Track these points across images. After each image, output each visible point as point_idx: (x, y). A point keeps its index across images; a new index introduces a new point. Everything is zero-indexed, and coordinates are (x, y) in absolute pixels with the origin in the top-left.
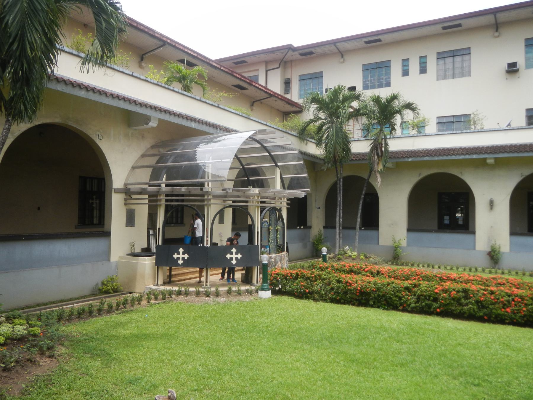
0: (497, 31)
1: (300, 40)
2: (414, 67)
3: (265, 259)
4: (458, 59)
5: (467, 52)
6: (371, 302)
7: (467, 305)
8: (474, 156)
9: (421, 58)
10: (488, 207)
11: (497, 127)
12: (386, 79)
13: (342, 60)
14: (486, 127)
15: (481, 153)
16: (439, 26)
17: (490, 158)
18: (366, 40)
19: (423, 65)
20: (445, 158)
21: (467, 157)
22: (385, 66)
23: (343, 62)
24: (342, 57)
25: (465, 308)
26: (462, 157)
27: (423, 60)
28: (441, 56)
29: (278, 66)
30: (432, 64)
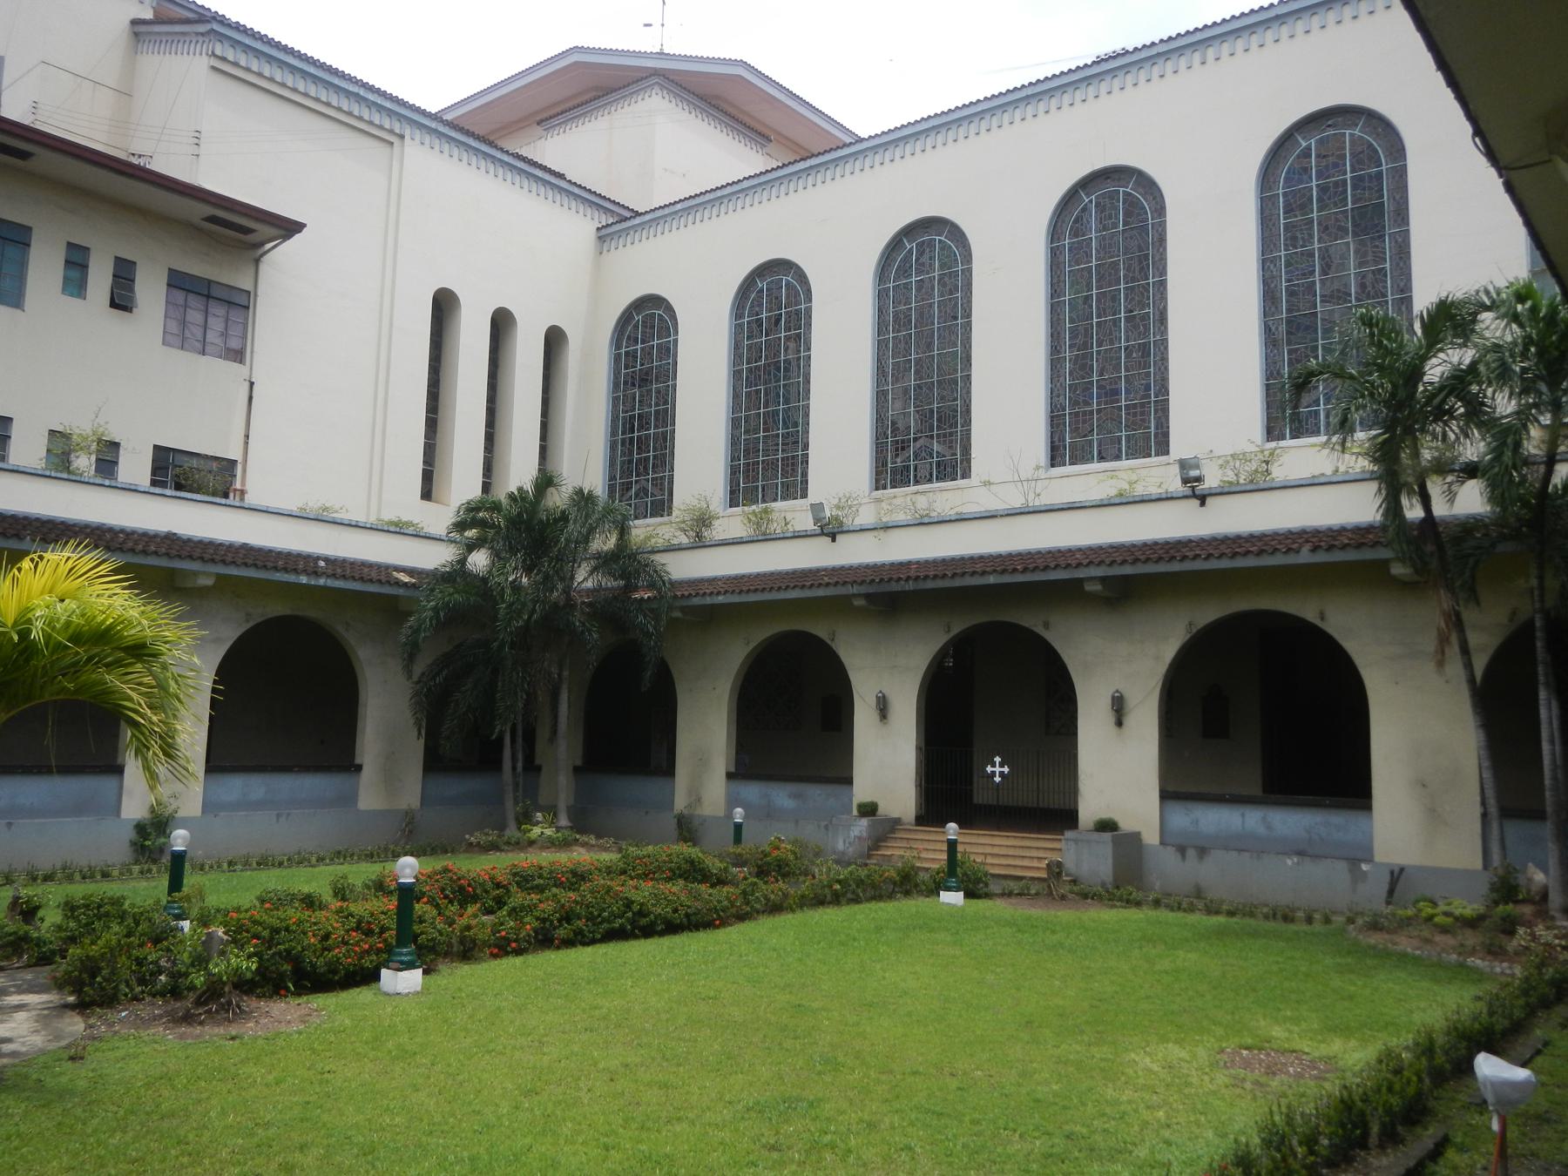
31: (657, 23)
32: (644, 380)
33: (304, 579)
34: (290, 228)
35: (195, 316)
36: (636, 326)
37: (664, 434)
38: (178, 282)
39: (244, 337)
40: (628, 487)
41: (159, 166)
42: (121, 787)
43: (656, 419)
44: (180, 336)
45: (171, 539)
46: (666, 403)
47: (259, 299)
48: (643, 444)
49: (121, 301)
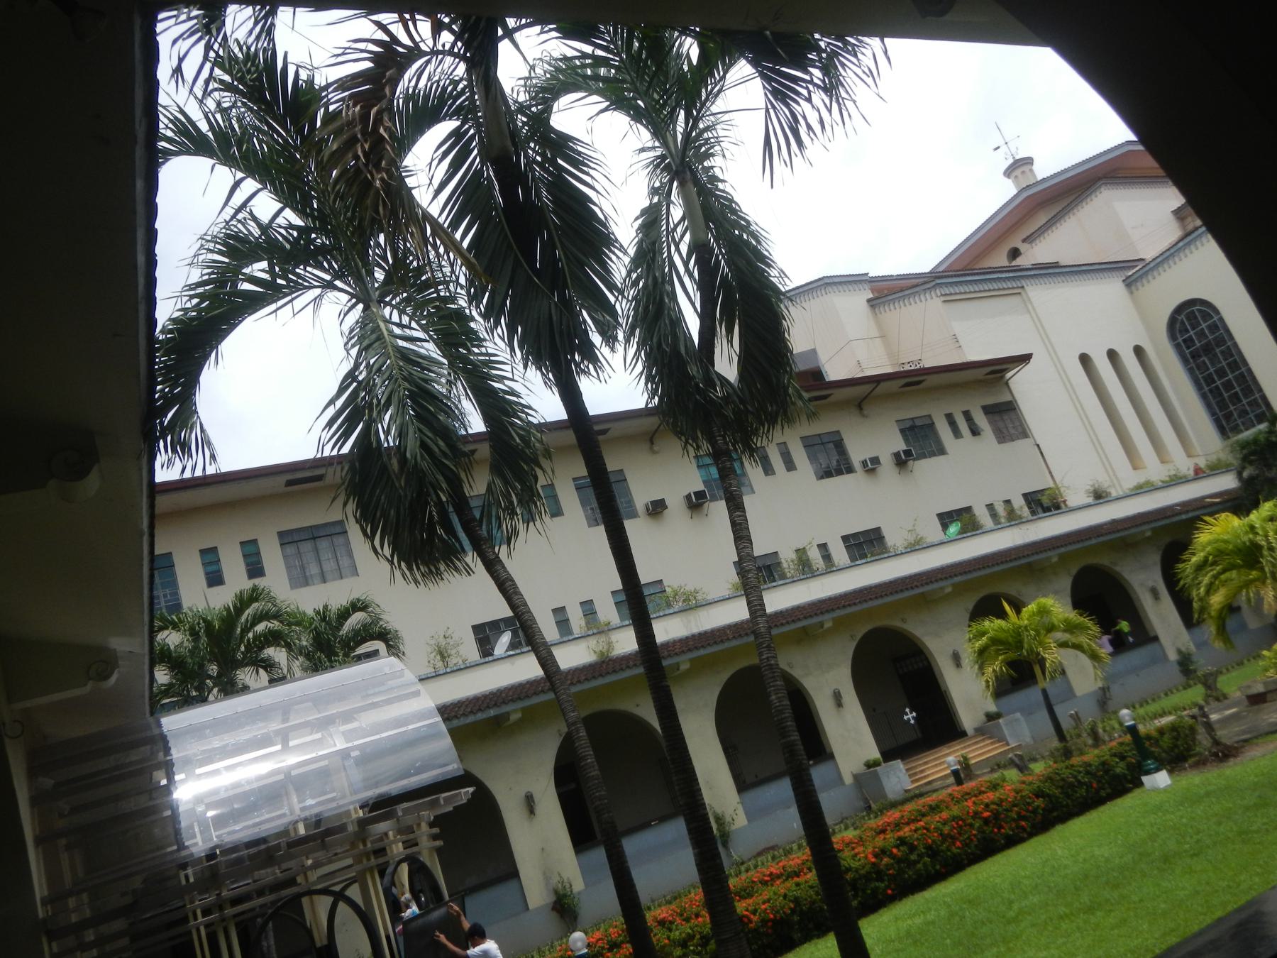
3: (579, 944)
4: (323, 544)
5: (338, 529)
6: (797, 936)
7: (915, 862)
10: (525, 812)
12: (165, 596)
15: (504, 703)
16: (283, 479)
17: (515, 711)
19: (254, 559)
21: (480, 716)
25: (920, 866)
26: (471, 719)
27: (251, 549)
28: (287, 539)
30: (272, 556)
31: (1001, 143)
32: (1207, 349)
33: (1184, 517)
34: (1025, 359)
35: (1001, 424)
36: (1182, 322)
37: (1242, 375)
38: (989, 410)
39: (1021, 425)
40: (1228, 417)
41: (928, 363)
42: (1161, 645)
43: (1230, 368)
44: (1002, 437)
45: (1114, 522)
46: (1232, 356)
47: (1019, 402)
48: (1228, 386)
49: (975, 432)
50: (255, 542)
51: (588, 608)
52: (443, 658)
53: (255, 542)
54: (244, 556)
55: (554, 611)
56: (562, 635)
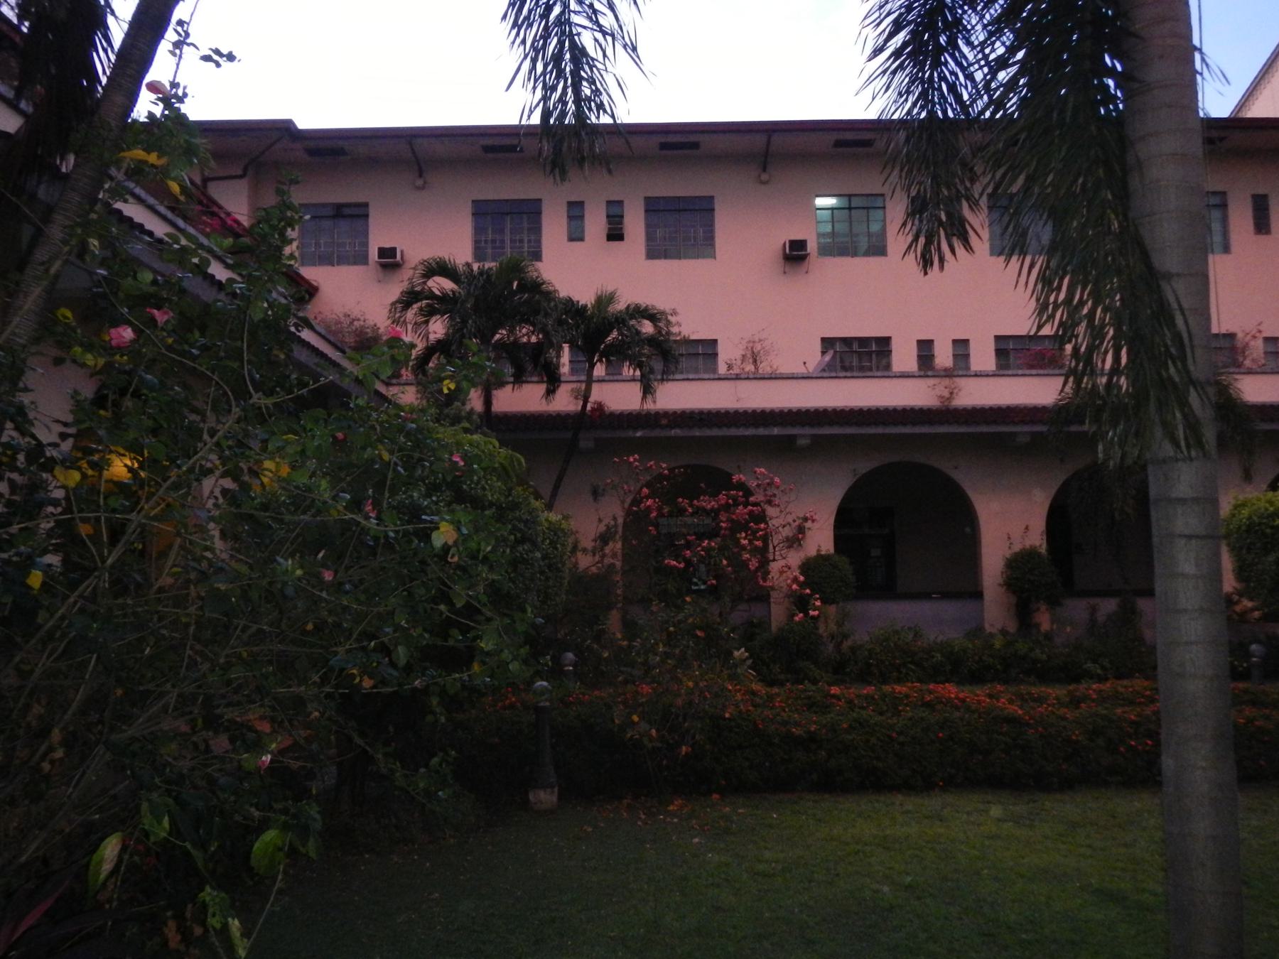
0: (764, 170)
1: (314, 114)
2: (596, 223)
8: (776, 431)
9: (609, 203)
11: (801, 370)
12: (529, 241)
13: (420, 182)
14: (785, 370)
17: (803, 436)
18: (489, 142)
20: (715, 432)
21: (762, 431)
22: (531, 212)
23: (422, 188)
24: (420, 176)
27: (615, 211)
28: (654, 207)
29: (240, 172)
30: (635, 224)
50: (620, 203)
51: (961, 345)
52: (755, 361)
53: (620, 203)
54: (608, 216)
55: (920, 342)
56: (920, 369)
